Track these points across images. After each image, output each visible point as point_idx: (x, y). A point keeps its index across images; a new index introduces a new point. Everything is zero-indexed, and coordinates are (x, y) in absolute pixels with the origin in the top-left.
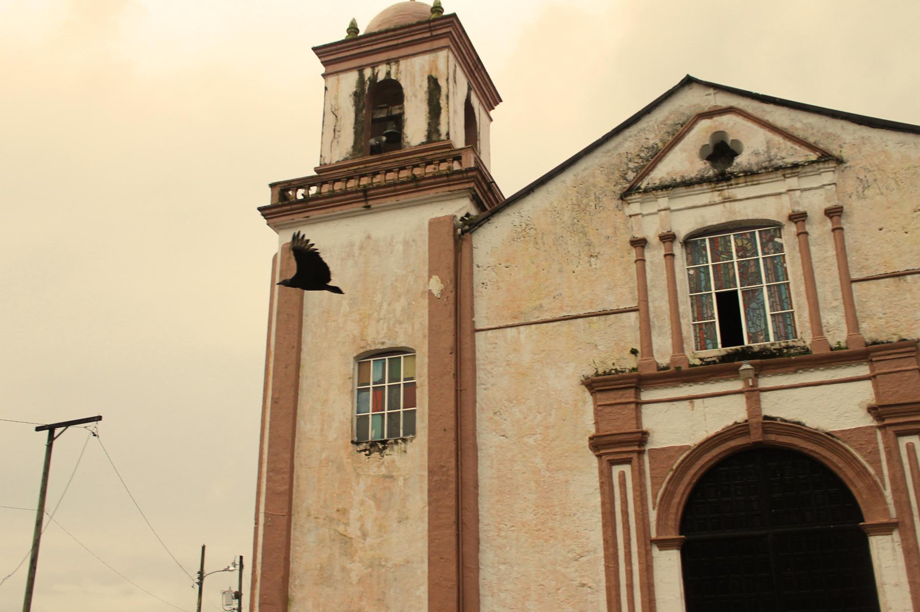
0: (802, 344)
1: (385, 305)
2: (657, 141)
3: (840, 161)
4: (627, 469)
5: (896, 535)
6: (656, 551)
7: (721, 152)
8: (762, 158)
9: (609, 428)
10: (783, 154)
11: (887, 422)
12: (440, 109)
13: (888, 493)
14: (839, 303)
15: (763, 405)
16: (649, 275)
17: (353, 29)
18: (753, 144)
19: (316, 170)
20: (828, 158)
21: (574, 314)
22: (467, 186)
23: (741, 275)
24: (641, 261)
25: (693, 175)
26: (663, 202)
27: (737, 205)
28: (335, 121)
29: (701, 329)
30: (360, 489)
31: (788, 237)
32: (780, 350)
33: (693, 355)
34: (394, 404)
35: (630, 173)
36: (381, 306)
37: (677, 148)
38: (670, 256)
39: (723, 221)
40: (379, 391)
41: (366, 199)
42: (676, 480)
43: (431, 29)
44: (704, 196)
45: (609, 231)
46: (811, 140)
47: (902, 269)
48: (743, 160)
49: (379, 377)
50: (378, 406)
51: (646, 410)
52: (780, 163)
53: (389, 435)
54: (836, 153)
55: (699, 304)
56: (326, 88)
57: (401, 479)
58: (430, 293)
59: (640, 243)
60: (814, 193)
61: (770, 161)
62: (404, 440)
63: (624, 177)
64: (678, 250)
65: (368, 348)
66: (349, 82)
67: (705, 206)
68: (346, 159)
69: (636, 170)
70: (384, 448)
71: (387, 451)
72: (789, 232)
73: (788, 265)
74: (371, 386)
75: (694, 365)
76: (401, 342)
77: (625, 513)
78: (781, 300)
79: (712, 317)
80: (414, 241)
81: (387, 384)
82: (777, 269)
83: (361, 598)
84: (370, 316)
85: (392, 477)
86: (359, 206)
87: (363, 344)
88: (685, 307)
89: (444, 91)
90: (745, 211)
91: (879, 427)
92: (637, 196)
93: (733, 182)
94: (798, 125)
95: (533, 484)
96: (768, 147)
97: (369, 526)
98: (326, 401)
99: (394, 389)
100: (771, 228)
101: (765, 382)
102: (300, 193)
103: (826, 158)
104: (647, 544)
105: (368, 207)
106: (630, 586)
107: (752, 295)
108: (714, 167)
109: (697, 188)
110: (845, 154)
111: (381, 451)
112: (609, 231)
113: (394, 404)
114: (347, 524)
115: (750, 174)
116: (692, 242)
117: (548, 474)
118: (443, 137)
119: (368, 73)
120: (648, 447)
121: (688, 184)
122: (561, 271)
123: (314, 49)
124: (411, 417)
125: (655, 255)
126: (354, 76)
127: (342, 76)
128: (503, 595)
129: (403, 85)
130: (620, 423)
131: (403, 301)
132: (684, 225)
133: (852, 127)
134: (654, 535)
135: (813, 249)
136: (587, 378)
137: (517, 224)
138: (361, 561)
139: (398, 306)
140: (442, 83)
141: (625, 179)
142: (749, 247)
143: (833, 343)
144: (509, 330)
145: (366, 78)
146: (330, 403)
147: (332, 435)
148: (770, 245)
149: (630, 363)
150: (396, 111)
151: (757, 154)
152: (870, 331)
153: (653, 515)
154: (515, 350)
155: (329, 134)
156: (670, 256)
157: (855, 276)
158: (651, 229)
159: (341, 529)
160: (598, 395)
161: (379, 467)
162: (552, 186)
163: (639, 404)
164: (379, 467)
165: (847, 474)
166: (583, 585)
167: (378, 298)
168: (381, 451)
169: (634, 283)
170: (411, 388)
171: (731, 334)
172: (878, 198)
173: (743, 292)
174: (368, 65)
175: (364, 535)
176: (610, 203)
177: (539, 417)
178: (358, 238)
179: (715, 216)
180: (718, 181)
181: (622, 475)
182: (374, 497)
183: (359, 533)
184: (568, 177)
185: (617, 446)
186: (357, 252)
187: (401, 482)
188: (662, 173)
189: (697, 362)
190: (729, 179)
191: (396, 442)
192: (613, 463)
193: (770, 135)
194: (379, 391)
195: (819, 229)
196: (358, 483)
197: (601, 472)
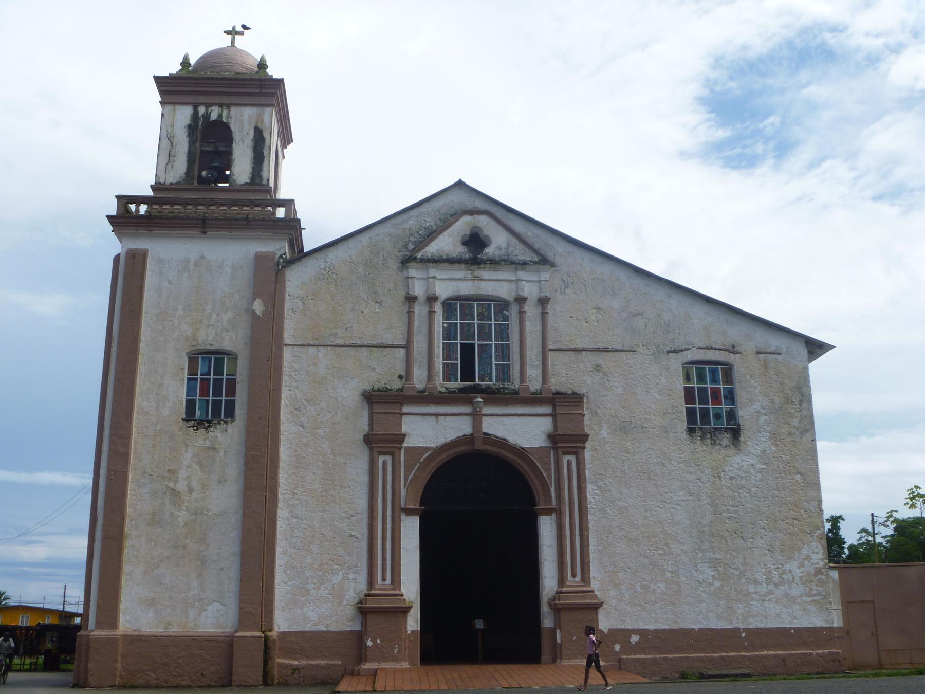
0: (512, 387)
1: (214, 316)
2: (432, 224)
3: (553, 265)
4: (389, 459)
5: (554, 515)
6: (403, 517)
7: (475, 241)
8: (503, 252)
9: (378, 430)
10: (517, 253)
11: (559, 445)
12: (263, 157)
13: (553, 490)
14: (539, 363)
15: (483, 425)
16: (416, 324)
17: (185, 63)
18: (499, 241)
19: (152, 187)
20: (544, 261)
21: (359, 343)
22: (289, 232)
24: (410, 313)
25: (455, 255)
27: (483, 284)
28: (169, 147)
29: (447, 367)
30: (188, 456)
31: (513, 312)
32: (499, 389)
33: (440, 383)
34: (217, 393)
35: (410, 244)
36: (211, 315)
37: (445, 233)
39: (472, 293)
41: (203, 226)
43: (261, 87)
44: (460, 272)
45: (391, 286)
46: (536, 246)
47: (580, 345)
48: (490, 251)
49: (206, 370)
50: (204, 393)
51: (405, 419)
52: (514, 258)
53: (213, 416)
54: (551, 259)
55: (448, 350)
56: (163, 115)
57: (222, 451)
58: (254, 312)
59: (411, 299)
61: (508, 255)
62: (226, 422)
63: (406, 246)
64: (438, 308)
65: (199, 347)
66: (184, 114)
67: (460, 279)
68: (179, 183)
69: (415, 243)
70: (209, 426)
71: (212, 429)
74: (199, 376)
75: (441, 392)
76: (227, 345)
77: (384, 488)
78: (503, 355)
80: (241, 267)
81: (212, 377)
82: (503, 333)
83: (186, 537)
84: (201, 322)
85: (215, 449)
86: (196, 232)
87: (194, 343)
88: (439, 351)
89: (267, 142)
91: (553, 448)
92: (415, 264)
93: (482, 266)
94: (530, 234)
95: (320, 464)
96: (508, 246)
97: (195, 484)
98: (161, 385)
99: (218, 382)
100: (502, 305)
101: (486, 410)
102: (143, 209)
103: (544, 261)
105: (204, 233)
107: (484, 349)
108: (470, 251)
109: (457, 265)
110: (558, 260)
111: (207, 428)
112: (391, 286)
113: (217, 393)
114: (176, 482)
115: (494, 263)
117: (332, 457)
118: (264, 182)
119: (202, 110)
120: (405, 445)
121: (450, 261)
122: (353, 310)
123: (156, 78)
124: (231, 406)
125: (420, 310)
126: (188, 111)
127: (178, 107)
128: (294, 540)
131: (230, 314)
132: (444, 290)
133: (563, 243)
134: (403, 506)
135: (528, 323)
136: (366, 391)
137: (322, 266)
138: (188, 509)
139: (226, 317)
140: (266, 135)
141: (406, 248)
142: (486, 314)
143: (532, 389)
144: (310, 348)
145: (200, 115)
146: (162, 388)
147: (166, 412)
148: (500, 315)
149: (396, 385)
150: (222, 148)
151: (499, 248)
152: (555, 384)
153: (403, 492)
154: (314, 364)
155: (164, 159)
156: (431, 312)
157: (551, 345)
159: (171, 485)
160: (375, 406)
161: (204, 440)
162: (351, 243)
163: (402, 414)
164: (204, 440)
166: (352, 536)
167: (209, 308)
168: (207, 428)
169: (405, 328)
170: (232, 384)
171: (468, 373)
172: (573, 296)
173: (479, 345)
174: (202, 104)
175: (191, 491)
176: (394, 265)
177: (329, 415)
178: (193, 257)
179: (466, 288)
180: (472, 264)
181: (385, 463)
182: (200, 463)
183: (186, 489)
184: (365, 238)
185: (382, 442)
186: (192, 268)
187: (222, 454)
188: (432, 249)
189: (443, 390)
190: (480, 264)
191: (219, 423)
192: (381, 453)
193: (510, 237)
194: (205, 382)
195: (531, 310)
196: (187, 452)
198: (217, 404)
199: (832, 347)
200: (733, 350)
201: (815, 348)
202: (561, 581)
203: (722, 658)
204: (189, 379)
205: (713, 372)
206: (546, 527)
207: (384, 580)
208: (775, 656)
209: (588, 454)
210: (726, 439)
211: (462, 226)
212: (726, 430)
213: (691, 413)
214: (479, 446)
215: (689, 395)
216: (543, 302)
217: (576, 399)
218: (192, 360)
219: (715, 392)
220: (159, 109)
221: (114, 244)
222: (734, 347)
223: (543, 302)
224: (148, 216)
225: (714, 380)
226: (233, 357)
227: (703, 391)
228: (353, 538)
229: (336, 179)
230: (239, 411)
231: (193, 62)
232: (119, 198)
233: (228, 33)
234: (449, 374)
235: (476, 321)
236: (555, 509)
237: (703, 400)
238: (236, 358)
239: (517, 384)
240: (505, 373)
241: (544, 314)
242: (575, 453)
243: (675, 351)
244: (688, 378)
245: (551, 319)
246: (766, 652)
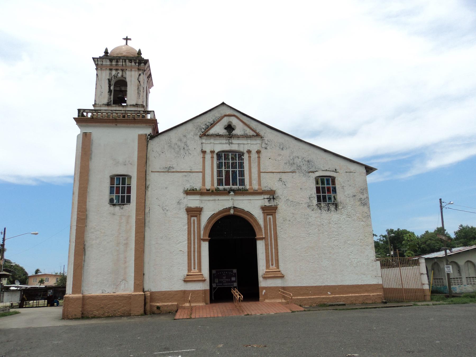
4: (195, 218)
5: (264, 240)
6: (202, 242)
7: (230, 128)
20: (258, 135)
24: (204, 158)
26: (212, 141)
31: (246, 157)
38: (212, 157)
49: (118, 183)
59: (204, 152)
60: (254, 145)
64: (215, 156)
66: (106, 75)
73: (245, 165)
74: (115, 186)
79: (223, 177)
82: (241, 165)
90: (234, 147)
100: (241, 154)
104: (200, 240)
106: (194, 251)
107: (234, 173)
115: (238, 137)
125: (208, 156)
129: (128, 80)
132: (218, 148)
134: (202, 238)
146: (100, 190)
150: (123, 89)
153: (202, 232)
158: (208, 148)
170: (129, 189)
173: (232, 171)
179: (226, 147)
185: (193, 212)
188: (212, 131)
192: (192, 216)
195: (254, 156)
197: (188, 219)
198: (123, 197)
199: (376, 169)
200: (336, 171)
201: (369, 170)
202: (268, 267)
203: (333, 297)
204: (111, 187)
205: (328, 181)
207: (194, 269)
208: (354, 296)
209: (277, 216)
210: (332, 208)
211: (225, 122)
212: (333, 204)
213: (319, 198)
215: (318, 189)
216: (258, 152)
218: (112, 178)
219: (329, 189)
220: (95, 72)
222: (336, 170)
223: (258, 152)
224: (92, 117)
225: (328, 184)
226: (130, 177)
227: (323, 188)
228: (182, 252)
229: (172, 101)
231: (109, 51)
232: (79, 110)
233: (124, 39)
234: (220, 182)
235: (230, 161)
236: (264, 238)
237: (324, 192)
238: (131, 178)
239: (248, 187)
240: (242, 182)
241: (259, 157)
242: (272, 215)
243: (312, 172)
244: (317, 183)
245: (262, 159)
246: (350, 295)
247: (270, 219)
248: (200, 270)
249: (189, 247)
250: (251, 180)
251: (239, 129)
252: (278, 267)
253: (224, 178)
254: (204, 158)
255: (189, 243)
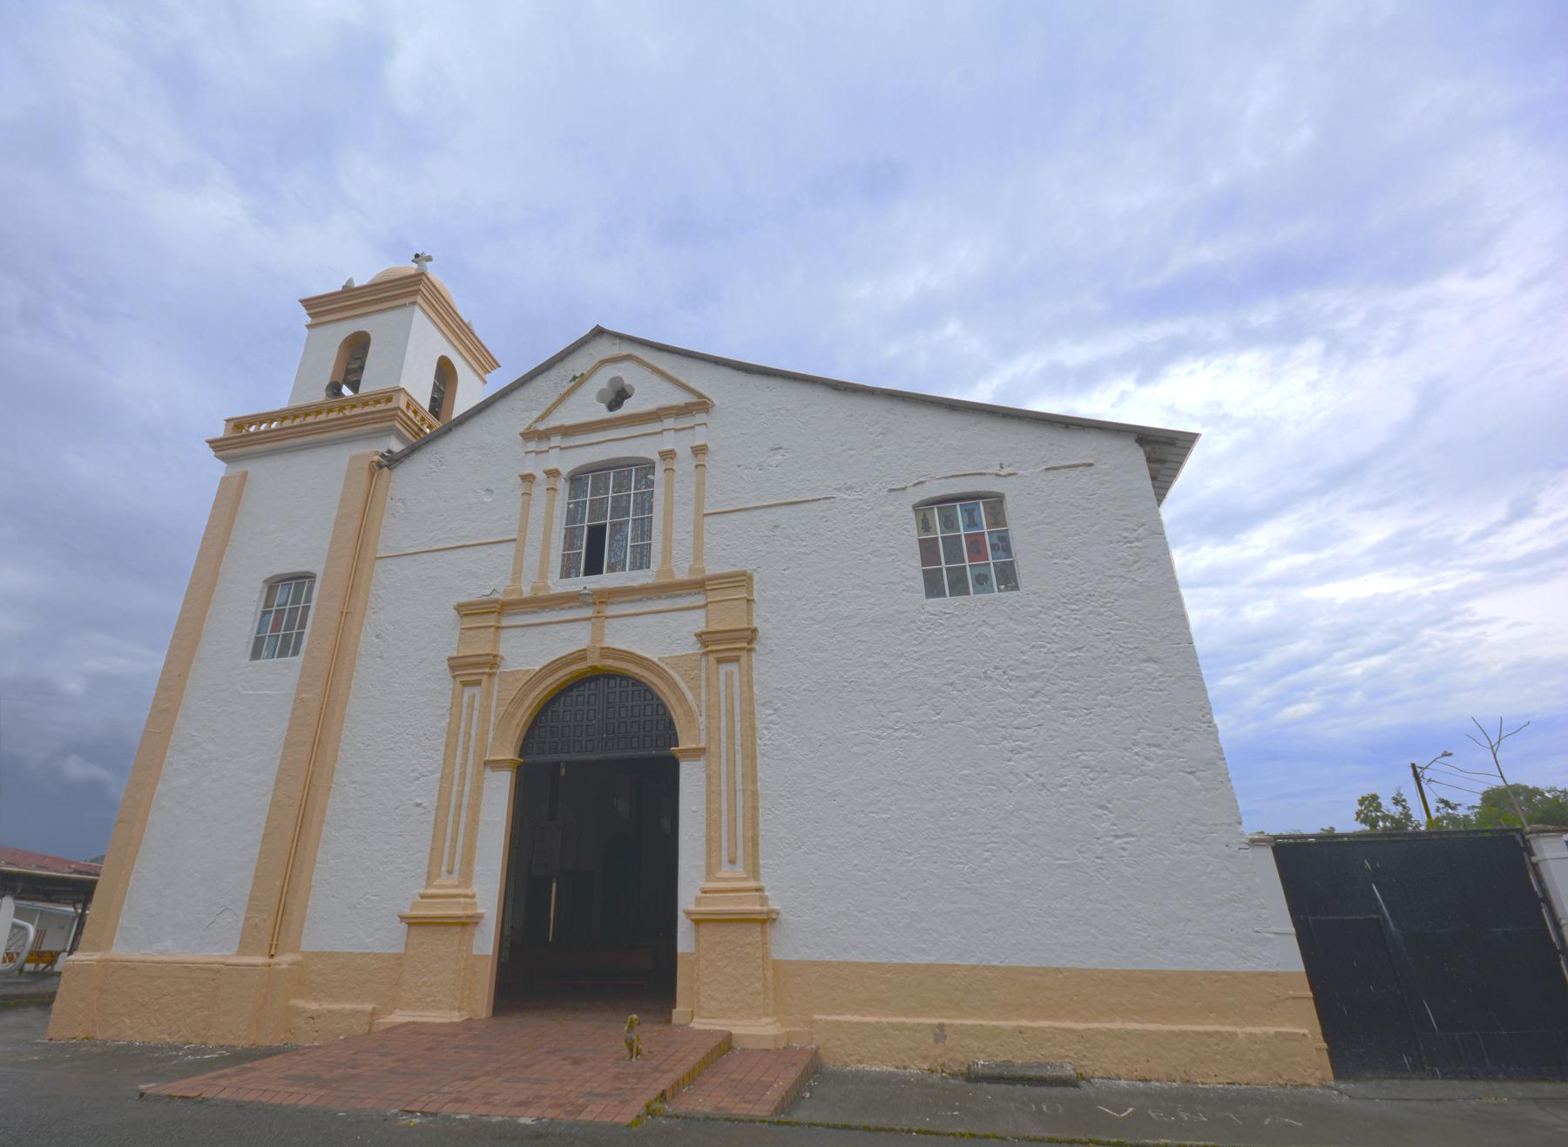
5: (702, 762)
6: (489, 773)
23: (613, 508)
24: (527, 494)
31: (659, 476)
34: (290, 626)
40: (280, 613)
42: (516, 702)
50: (276, 628)
55: (571, 537)
59: (528, 478)
64: (563, 487)
72: (659, 468)
82: (645, 503)
100: (646, 467)
107: (618, 527)
113: (290, 626)
116: (576, 479)
130: (480, 646)
132: (569, 460)
165: (670, 700)
185: (471, 670)
192: (465, 684)
194: (280, 613)
195: (684, 464)
202: (710, 872)
206: (691, 779)
211: (602, 380)
214: (594, 661)
217: (742, 580)
221: (219, 469)
228: (420, 810)
230: (303, 647)
247: (729, 676)
248: (466, 878)
249: (444, 794)
250: (676, 547)
251: (647, 394)
252: (755, 872)
253: (584, 551)
254: (527, 494)
255: (446, 777)
